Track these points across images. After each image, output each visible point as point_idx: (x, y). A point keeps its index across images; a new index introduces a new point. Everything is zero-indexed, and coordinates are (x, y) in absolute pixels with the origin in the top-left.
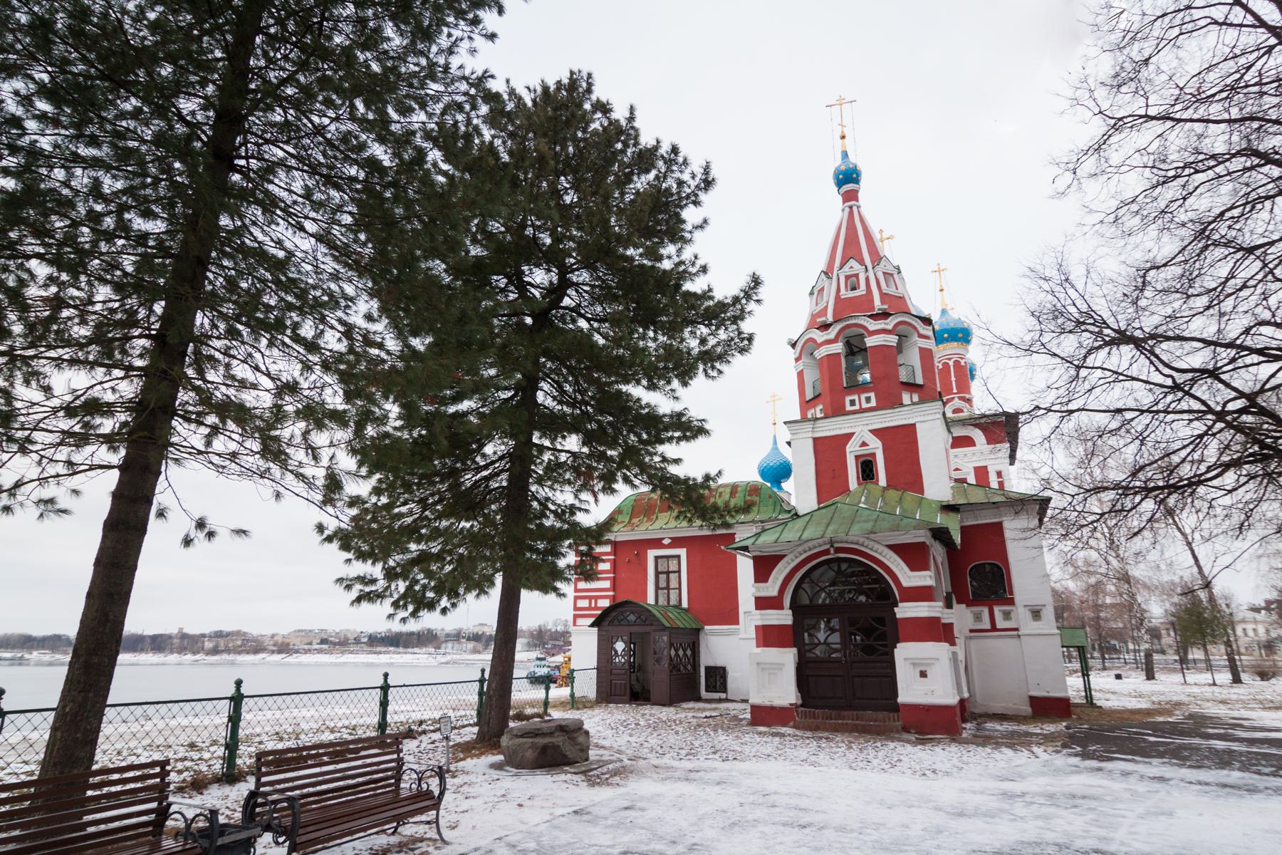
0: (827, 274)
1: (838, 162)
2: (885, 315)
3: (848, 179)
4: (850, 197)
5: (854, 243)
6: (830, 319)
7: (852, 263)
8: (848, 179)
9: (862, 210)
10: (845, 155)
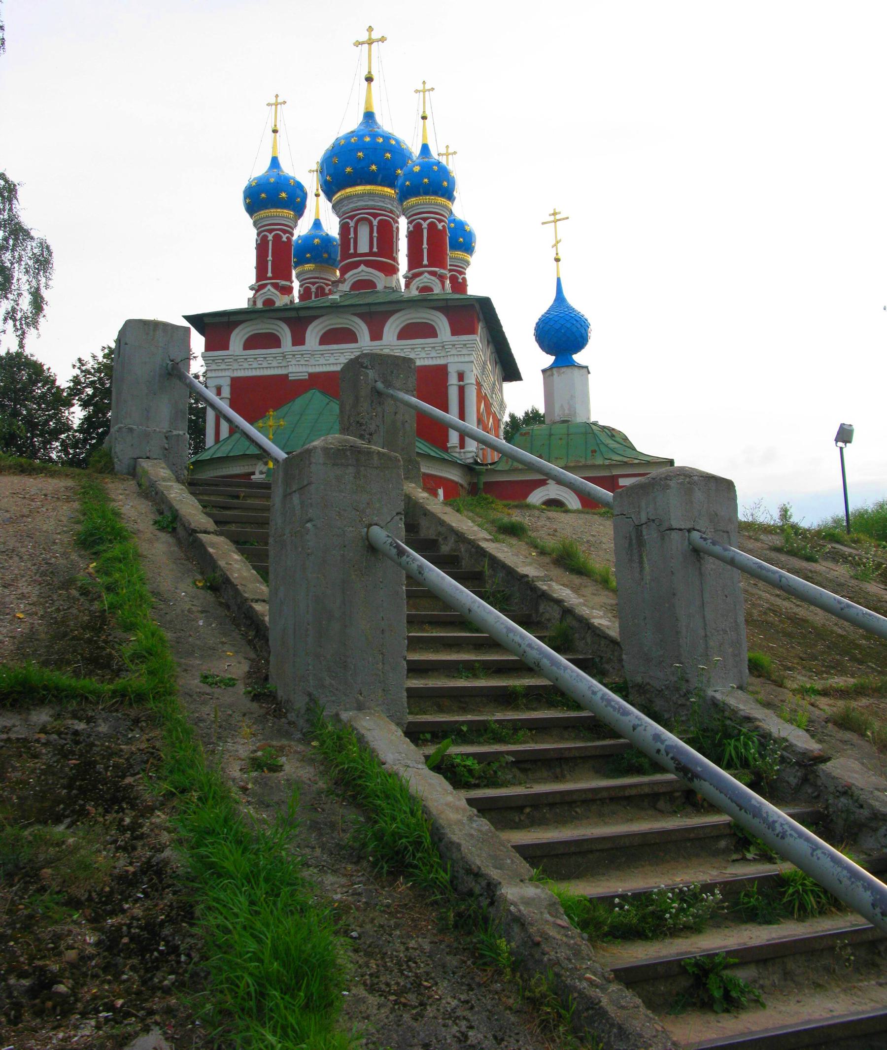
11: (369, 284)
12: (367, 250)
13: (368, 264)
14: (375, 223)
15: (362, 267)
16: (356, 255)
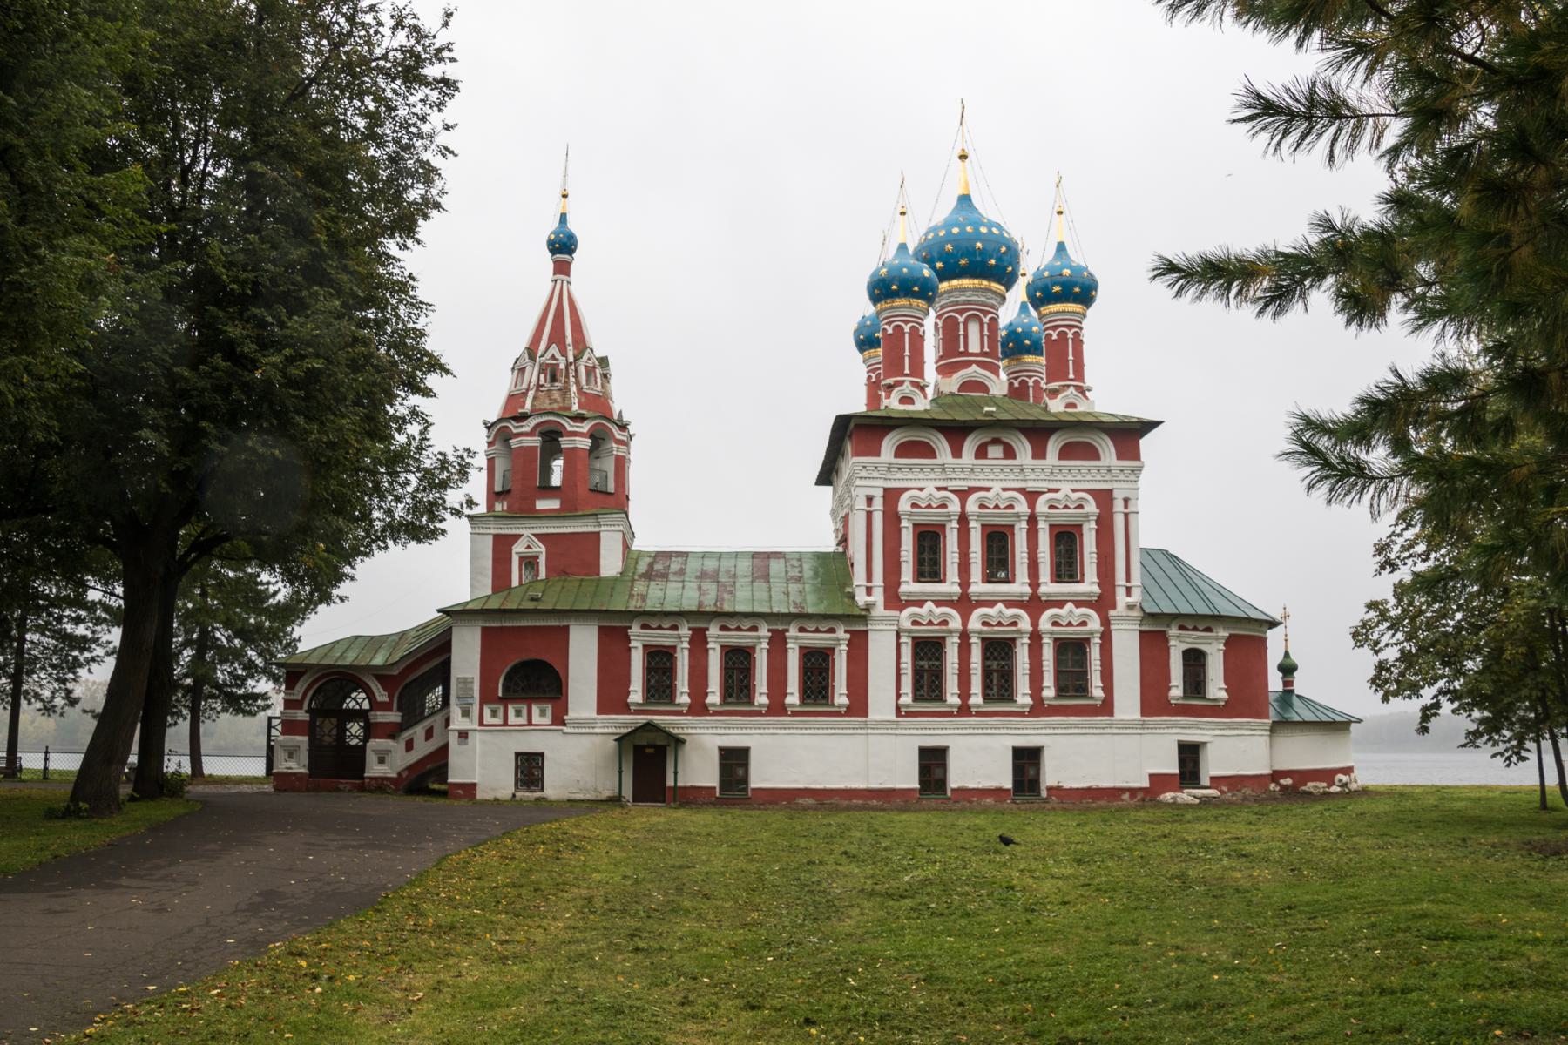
0: (531, 351)
1: (554, 224)
2: (580, 418)
3: (563, 246)
4: (562, 269)
5: (560, 327)
6: (528, 407)
7: (554, 350)
8: (563, 246)
9: (572, 288)
10: (563, 218)
11: (983, 387)
12: (977, 350)
13: (982, 365)
14: (986, 320)
15: (974, 367)
16: (966, 353)
